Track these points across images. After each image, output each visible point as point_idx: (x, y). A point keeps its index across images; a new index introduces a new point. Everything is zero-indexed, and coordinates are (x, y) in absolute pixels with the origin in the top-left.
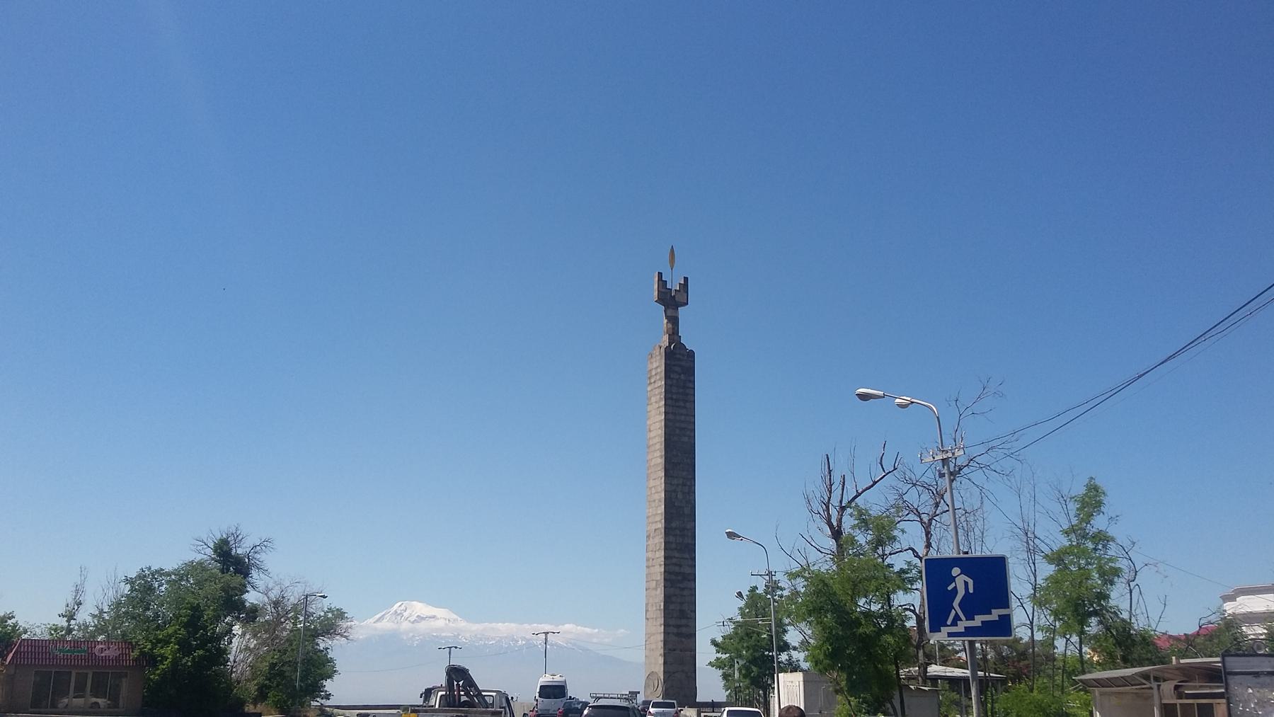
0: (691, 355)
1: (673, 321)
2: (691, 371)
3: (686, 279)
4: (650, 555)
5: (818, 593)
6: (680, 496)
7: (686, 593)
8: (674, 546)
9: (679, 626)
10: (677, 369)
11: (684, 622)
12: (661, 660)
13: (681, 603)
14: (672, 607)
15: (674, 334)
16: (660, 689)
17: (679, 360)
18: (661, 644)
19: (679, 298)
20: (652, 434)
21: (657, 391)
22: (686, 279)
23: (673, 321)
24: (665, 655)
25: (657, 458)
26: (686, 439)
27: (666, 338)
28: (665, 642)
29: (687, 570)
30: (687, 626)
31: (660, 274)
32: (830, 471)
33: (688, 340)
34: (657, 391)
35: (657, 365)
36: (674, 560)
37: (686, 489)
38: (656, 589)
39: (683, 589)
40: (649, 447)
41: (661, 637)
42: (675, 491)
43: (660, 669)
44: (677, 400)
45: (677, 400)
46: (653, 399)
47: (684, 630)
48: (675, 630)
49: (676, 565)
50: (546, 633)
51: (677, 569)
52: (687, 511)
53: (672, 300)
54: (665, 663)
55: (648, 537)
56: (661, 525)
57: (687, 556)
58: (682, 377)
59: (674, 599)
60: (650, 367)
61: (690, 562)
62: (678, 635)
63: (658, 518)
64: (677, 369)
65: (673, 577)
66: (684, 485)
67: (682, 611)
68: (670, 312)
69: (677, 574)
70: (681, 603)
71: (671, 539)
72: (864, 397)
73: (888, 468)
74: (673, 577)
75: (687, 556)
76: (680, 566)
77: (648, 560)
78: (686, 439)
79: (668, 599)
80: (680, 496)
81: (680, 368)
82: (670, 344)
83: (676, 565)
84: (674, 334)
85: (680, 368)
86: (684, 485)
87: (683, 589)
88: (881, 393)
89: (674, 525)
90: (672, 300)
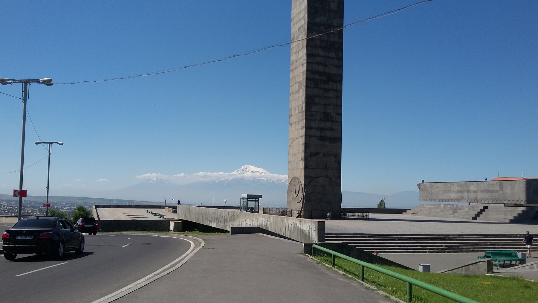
7: (331, 94)
9: (321, 129)
11: (328, 125)
12: (302, 165)
14: (314, 109)
16: (301, 194)
18: (302, 148)
29: (334, 71)
30: (331, 129)
36: (318, 59)
38: (298, 92)
39: (327, 90)
41: (302, 140)
43: (300, 174)
47: (328, 134)
48: (318, 133)
49: (317, 63)
51: (321, 68)
54: (306, 167)
59: (317, 100)
62: (322, 138)
65: (317, 77)
74: (317, 77)
75: (333, 55)
76: (325, 65)
79: (310, 101)
83: (317, 63)
87: (327, 90)
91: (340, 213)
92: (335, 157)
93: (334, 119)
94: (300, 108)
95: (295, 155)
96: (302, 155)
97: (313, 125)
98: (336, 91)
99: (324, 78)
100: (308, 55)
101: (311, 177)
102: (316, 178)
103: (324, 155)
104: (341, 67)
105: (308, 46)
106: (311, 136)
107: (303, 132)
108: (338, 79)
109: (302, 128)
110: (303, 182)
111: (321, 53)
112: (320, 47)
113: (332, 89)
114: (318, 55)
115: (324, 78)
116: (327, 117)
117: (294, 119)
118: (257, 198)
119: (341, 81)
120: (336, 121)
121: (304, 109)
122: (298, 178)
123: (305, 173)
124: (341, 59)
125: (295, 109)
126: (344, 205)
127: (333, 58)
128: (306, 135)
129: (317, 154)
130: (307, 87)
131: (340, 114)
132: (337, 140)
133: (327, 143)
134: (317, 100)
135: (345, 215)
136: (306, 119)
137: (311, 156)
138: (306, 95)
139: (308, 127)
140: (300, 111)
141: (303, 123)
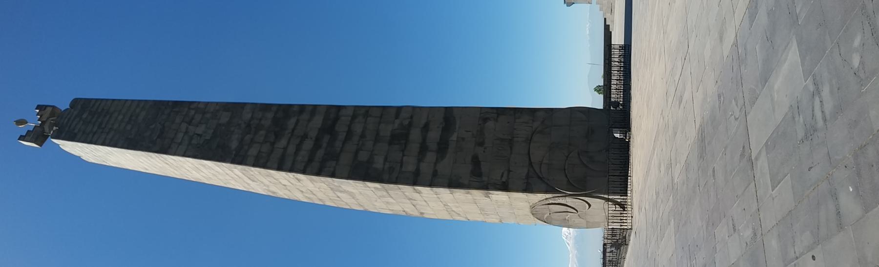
6: (200, 130)
7: (358, 128)
9: (423, 149)
11: (415, 135)
12: (499, 196)
13: (377, 139)
14: (379, 163)
18: (460, 194)
24: (486, 186)
28: (454, 184)
29: (318, 121)
30: (426, 128)
36: (291, 149)
37: (198, 117)
39: (349, 133)
42: (191, 138)
47: (434, 135)
48: (431, 157)
49: (298, 149)
51: (308, 145)
52: (225, 118)
54: (505, 187)
57: (293, 121)
61: (305, 116)
62: (442, 148)
65: (320, 153)
69: (317, 145)
70: (377, 139)
71: (253, 151)
74: (320, 153)
75: (293, 121)
76: (305, 137)
80: (200, 130)
83: (298, 149)
87: (349, 133)
89: (234, 145)
91: (616, 114)
92: (485, 120)
93: (406, 122)
94: (379, 193)
95: (482, 209)
96: (477, 194)
97: (410, 167)
98: (354, 117)
99: (326, 138)
100: (280, 168)
101: (528, 177)
102: (531, 164)
103: (481, 144)
104: (315, 107)
105: (264, 166)
106: (435, 174)
107: (426, 191)
108: (334, 114)
109: (419, 193)
110: (541, 196)
111: (283, 143)
112: (273, 144)
113: (349, 126)
114: (285, 149)
115: (326, 138)
116: (400, 138)
119: (339, 108)
120: (412, 117)
121: (377, 185)
122: (533, 207)
123: (517, 191)
124: (302, 108)
125: (388, 203)
126: (596, 102)
127: (298, 121)
128: (431, 185)
129: (476, 162)
130: (333, 175)
131: (399, 109)
132: (449, 115)
133: (454, 137)
134: (363, 156)
135: (616, 104)
136: (396, 182)
137: (480, 175)
138: (347, 178)
140: (385, 193)
141: (407, 190)
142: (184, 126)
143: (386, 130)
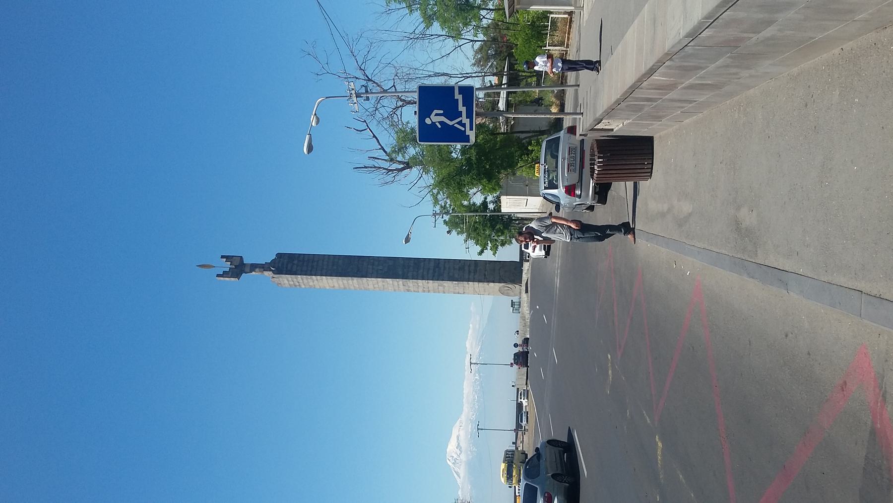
0: (280, 256)
1: (254, 267)
2: (291, 257)
3: (223, 257)
4: (421, 289)
5: (448, 185)
6: (380, 267)
7: (447, 266)
8: (415, 273)
9: (470, 272)
10: (289, 266)
11: (466, 268)
12: (492, 284)
13: (454, 269)
14: (456, 276)
15: (264, 267)
16: (510, 286)
17: (283, 264)
18: (481, 284)
19: (237, 263)
20: (336, 285)
21: (305, 281)
22: (223, 257)
23: (254, 267)
25: (353, 283)
26: (341, 262)
27: (266, 273)
28: (479, 281)
29: (432, 264)
30: (469, 266)
31: (218, 276)
32: (366, 167)
33: (269, 257)
34: (305, 281)
35: (286, 280)
36: (425, 273)
37: (376, 263)
39: (445, 268)
40: (345, 288)
43: (497, 286)
44: (312, 267)
45: (312, 267)
46: (311, 284)
47: (472, 268)
50: (471, 363)
51: (431, 271)
52: (391, 263)
53: (238, 268)
55: (408, 290)
56: (401, 281)
58: (296, 262)
59: (451, 274)
60: (287, 285)
62: (475, 271)
63: (396, 283)
64: (289, 266)
66: (373, 264)
67: (460, 269)
68: (247, 269)
69: (434, 272)
71: (410, 274)
72: (310, 148)
73: (364, 126)
77: (424, 291)
78: (341, 262)
79: (451, 279)
81: (289, 264)
82: (271, 270)
84: (264, 267)
85: (289, 264)
86: (373, 264)
87: (445, 268)
88: (307, 136)
90: (238, 268)
117: (461, 291)
118: (513, 304)
134: (451, 274)
139: (468, 280)
142: (370, 267)
143: (457, 267)
